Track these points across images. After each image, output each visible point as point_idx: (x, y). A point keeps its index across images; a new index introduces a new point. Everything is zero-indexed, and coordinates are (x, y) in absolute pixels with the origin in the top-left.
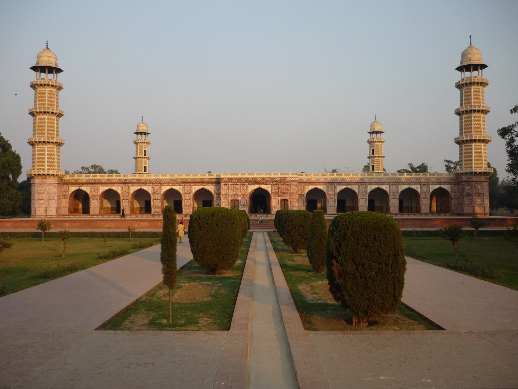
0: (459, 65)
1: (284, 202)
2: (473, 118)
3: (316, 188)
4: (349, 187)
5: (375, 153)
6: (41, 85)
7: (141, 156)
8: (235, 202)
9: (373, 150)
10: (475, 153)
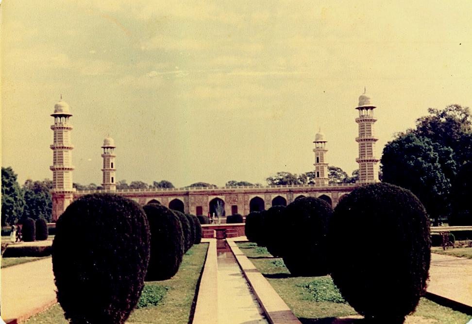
0: (358, 107)
1: (235, 208)
2: (366, 145)
3: (257, 197)
4: (281, 195)
5: (319, 161)
6: (60, 128)
7: (109, 168)
8: (199, 210)
9: (318, 158)
10: (368, 169)
